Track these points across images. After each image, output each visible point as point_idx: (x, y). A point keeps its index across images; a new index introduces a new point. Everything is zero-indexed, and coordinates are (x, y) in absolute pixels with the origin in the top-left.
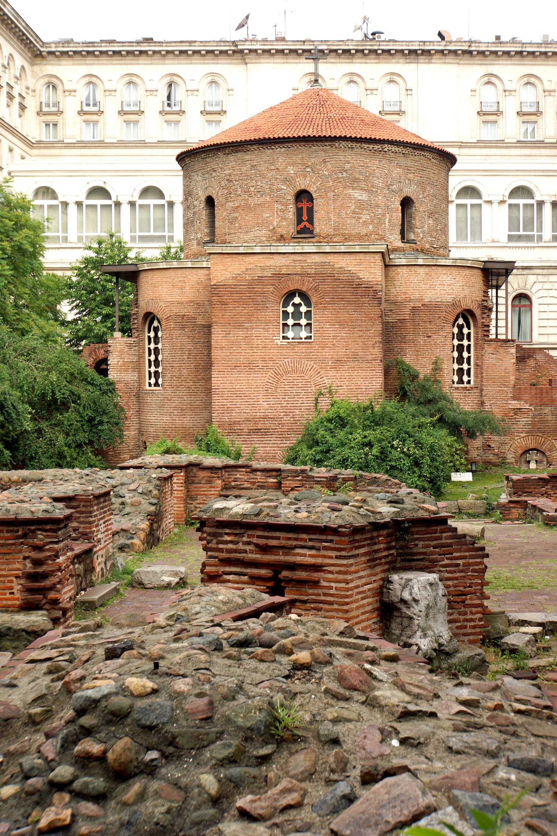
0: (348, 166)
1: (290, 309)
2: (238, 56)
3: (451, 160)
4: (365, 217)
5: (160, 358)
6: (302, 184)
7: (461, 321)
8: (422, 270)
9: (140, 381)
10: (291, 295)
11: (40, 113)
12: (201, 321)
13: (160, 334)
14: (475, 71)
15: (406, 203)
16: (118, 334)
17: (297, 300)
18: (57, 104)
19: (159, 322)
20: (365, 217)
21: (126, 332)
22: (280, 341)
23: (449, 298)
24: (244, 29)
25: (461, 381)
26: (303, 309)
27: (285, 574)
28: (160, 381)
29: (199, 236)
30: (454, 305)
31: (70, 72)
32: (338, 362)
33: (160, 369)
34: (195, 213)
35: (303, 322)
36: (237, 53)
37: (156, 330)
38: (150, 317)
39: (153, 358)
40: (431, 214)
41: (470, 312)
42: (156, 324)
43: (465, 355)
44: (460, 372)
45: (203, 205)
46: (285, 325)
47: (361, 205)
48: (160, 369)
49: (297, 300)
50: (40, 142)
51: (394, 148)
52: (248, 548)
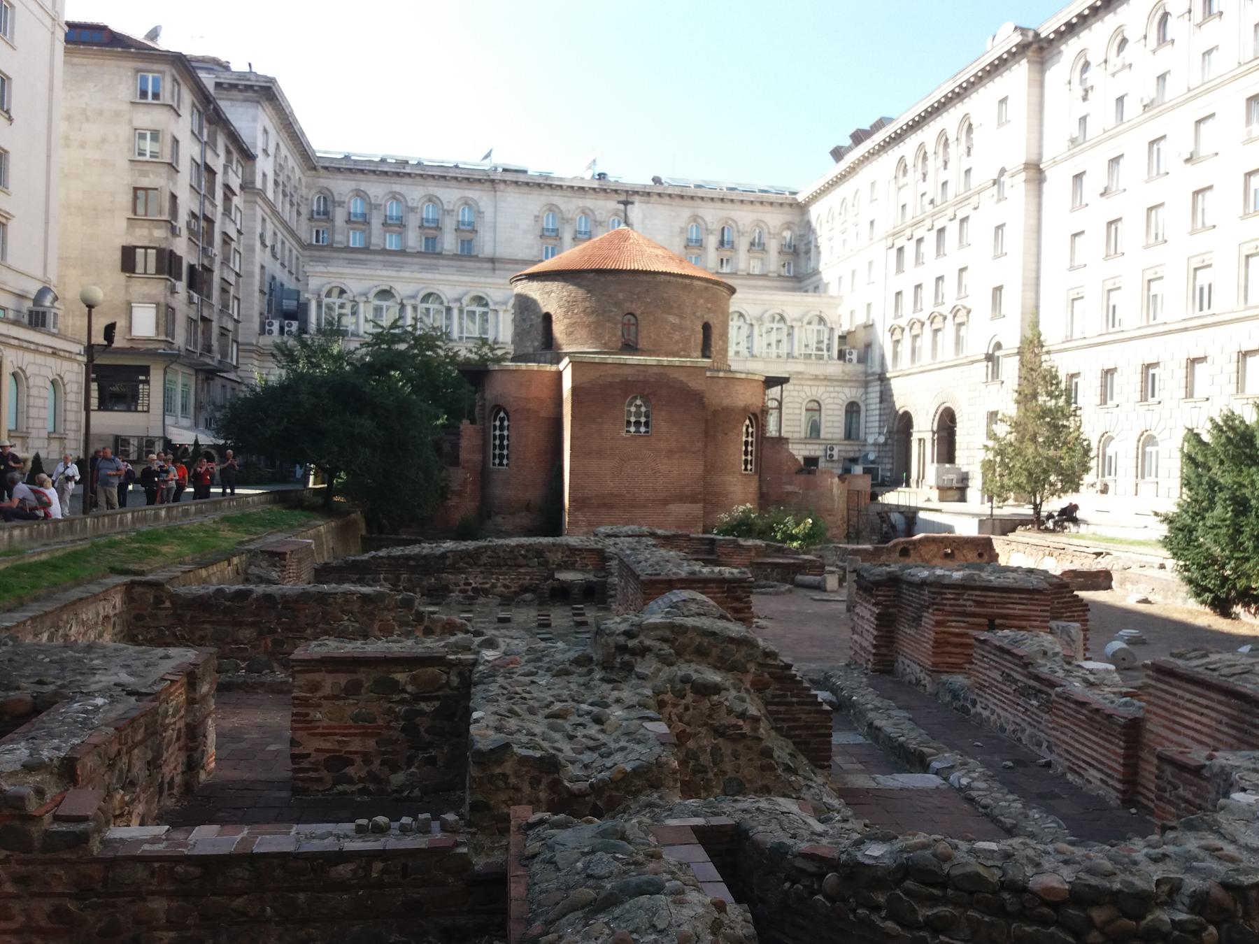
0: (665, 295)
1: (633, 409)
2: (488, 184)
3: (732, 291)
4: (677, 337)
5: (505, 442)
6: (629, 306)
7: (747, 422)
8: (721, 381)
9: (484, 462)
10: (635, 398)
11: (311, 219)
12: (543, 414)
13: (506, 423)
14: (684, 213)
15: (707, 328)
16: (466, 422)
17: (638, 402)
18: (326, 213)
19: (506, 413)
20: (677, 337)
21: (473, 422)
22: (624, 434)
23: (741, 404)
24: (487, 161)
25: (746, 469)
26: (643, 409)
27: (998, 621)
28: (505, 462)
29: (536, 344)
30: (745, 409)
31: (341, 187)
32: (670, 452)
33: (505, 452)
34: (531, 326)
35: (643, 420)
36: (489, 181)
37: (502, 420)
38: (498, 408)
39: (497, 442)
40: (721, 338)
41: (755, 415)
42: (502, 414)
43: (750, 448)
44: (746, 462)
45: (540, 320)
46: (629, 423)
47: (674, 326)
48: (505, 452)
49: (638, 402)
50: (311, 245)
51: (699, 283)
52: (968, 603)
